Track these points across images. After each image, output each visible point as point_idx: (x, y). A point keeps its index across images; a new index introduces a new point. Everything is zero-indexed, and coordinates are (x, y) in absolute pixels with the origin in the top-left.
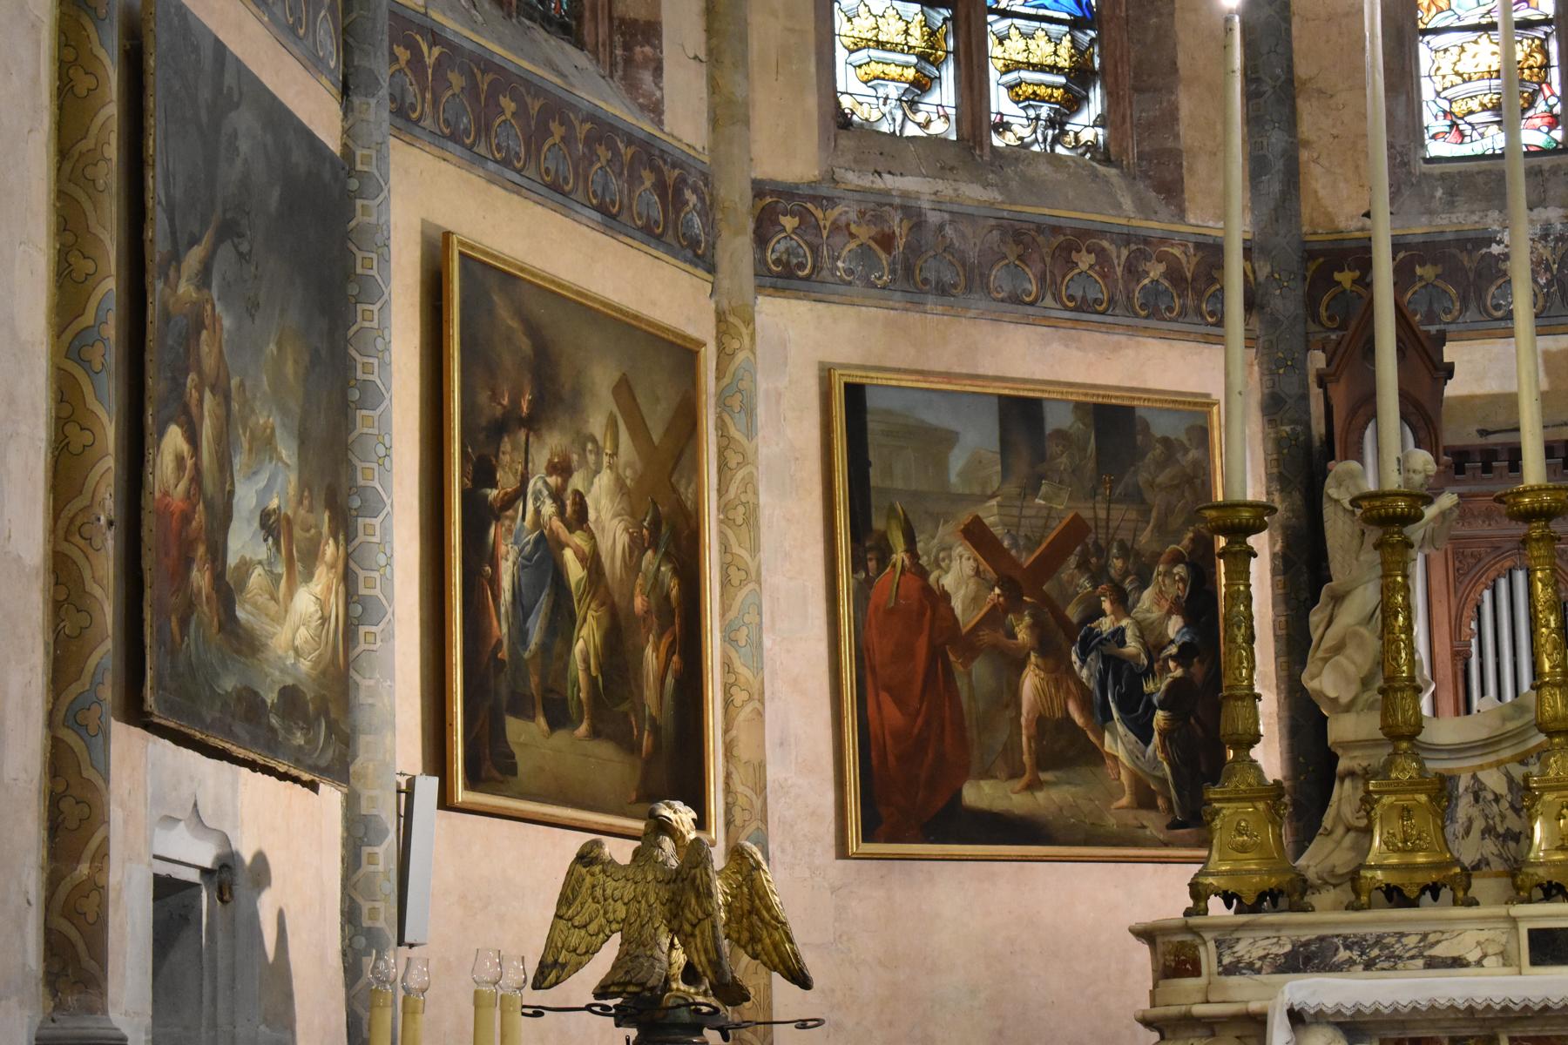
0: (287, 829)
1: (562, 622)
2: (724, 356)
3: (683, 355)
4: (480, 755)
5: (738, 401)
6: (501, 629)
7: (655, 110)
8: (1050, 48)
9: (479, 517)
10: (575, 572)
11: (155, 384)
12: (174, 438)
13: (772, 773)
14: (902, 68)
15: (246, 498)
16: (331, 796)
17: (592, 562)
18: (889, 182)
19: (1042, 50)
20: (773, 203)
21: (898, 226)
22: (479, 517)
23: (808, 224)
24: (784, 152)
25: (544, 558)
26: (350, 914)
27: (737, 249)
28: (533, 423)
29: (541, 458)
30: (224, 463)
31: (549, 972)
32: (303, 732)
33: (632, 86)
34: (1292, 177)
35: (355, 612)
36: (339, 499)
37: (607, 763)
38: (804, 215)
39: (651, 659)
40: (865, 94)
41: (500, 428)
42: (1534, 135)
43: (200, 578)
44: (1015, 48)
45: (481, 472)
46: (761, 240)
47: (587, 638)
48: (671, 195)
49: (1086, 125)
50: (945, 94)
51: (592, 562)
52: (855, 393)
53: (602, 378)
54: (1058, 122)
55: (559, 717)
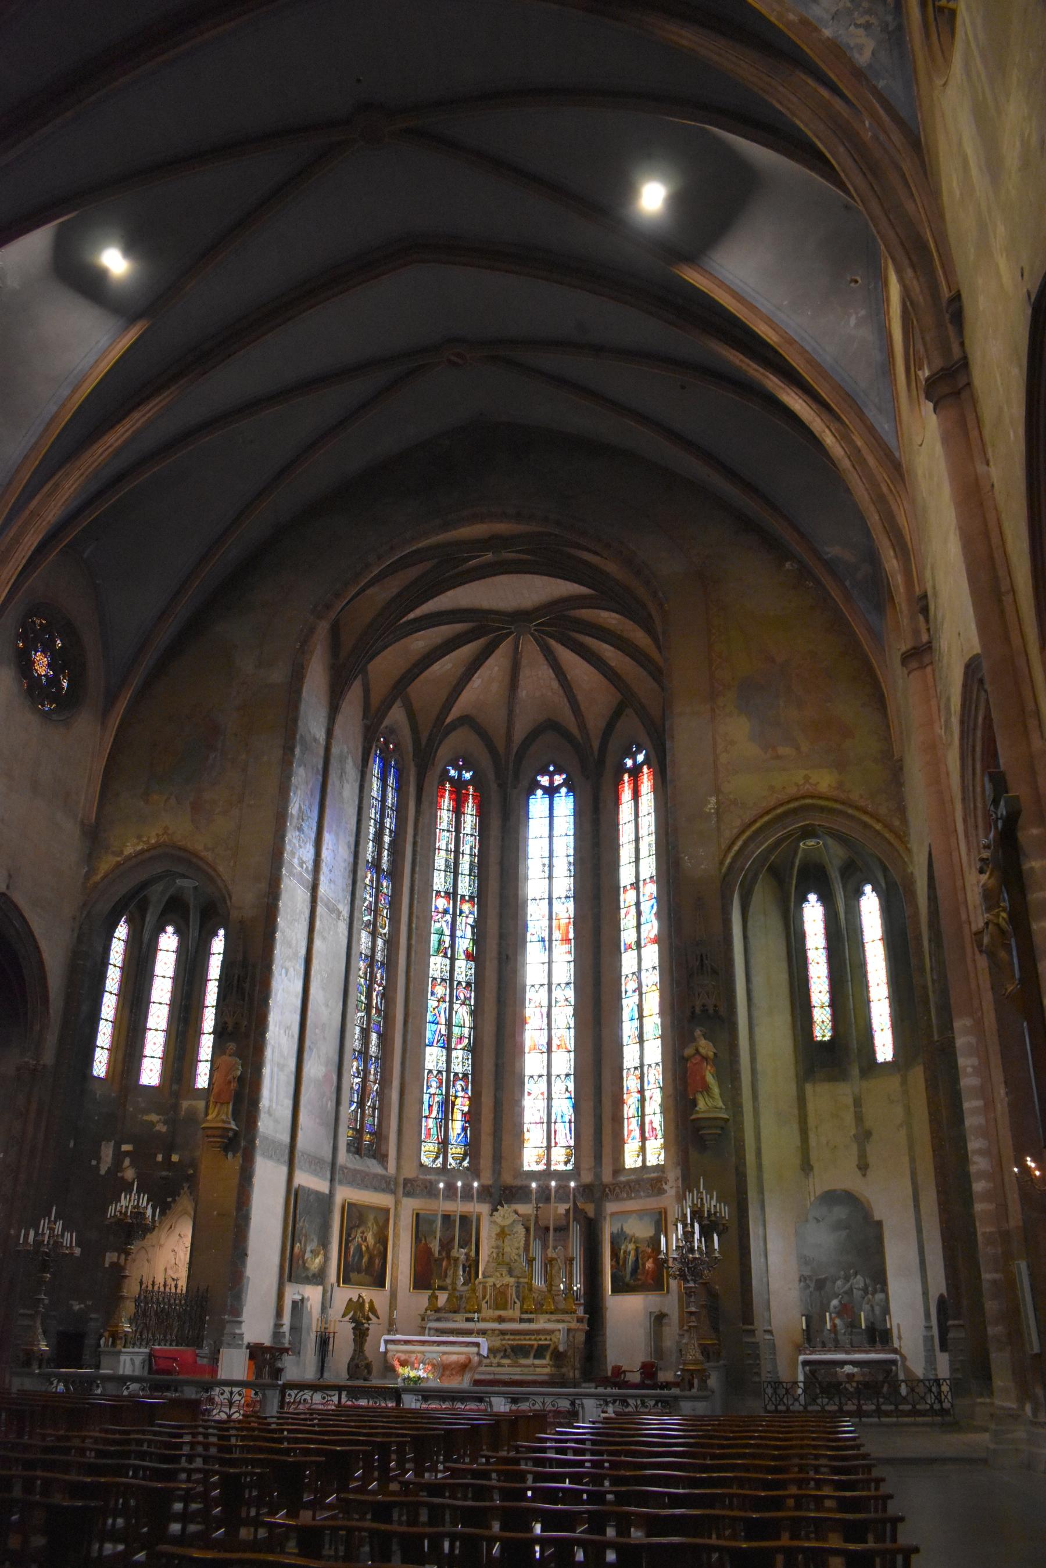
0: (313, 1294)
1: (361, 1256)
2: (396, 1209)
3: (388, 1211)
4: (345, 1279)
5: (397, 1216)
6: (350, 1259)
7: (386, 1169)
8: (460, 1150)
9: (348, 1242)
10: (364, 1248)
11: (296, 1239)
12: (298, 1244)
13: (399, 1277)
14: (433, 1155)
15: (308, 1249)
16: (320, 1288)
17: (367, 1247)
18: (428, 1177)
19: (458, 1150)
20: (406, 1181)
21: (428, 1185)
22: (348, 1242)
23: (412, 1185)
24: (409, 1172)
25: (359, 1246)
26: (323, 1304)
27: (401, 1190)
28: (358, 1226)
29: (360, 1231)
30: (305, 1246)
31: (343, 1316)
32: (318, 1278)
33: (383, 1166)
34: (499, 1174)
35: (327, 1259)
36: (324, 1243)
37: (368, 1279)
38: (412, 1185)
39: (377, 1261)
40: (426, 1160)
41: (352, 1228)
42: (542, 1167)
43: (301, 1262)
44: (454, 1151)
45: (349, 1235)
46: (404, 1188)
47: (365, 1260)
48: (388, 1183)
49: (466, 1164)
50: (441, 1159)
51: (367, 1247)
52: (418, 1215)
53: (371, 1217)
54: (460, 1163)
55: (359, 1272)
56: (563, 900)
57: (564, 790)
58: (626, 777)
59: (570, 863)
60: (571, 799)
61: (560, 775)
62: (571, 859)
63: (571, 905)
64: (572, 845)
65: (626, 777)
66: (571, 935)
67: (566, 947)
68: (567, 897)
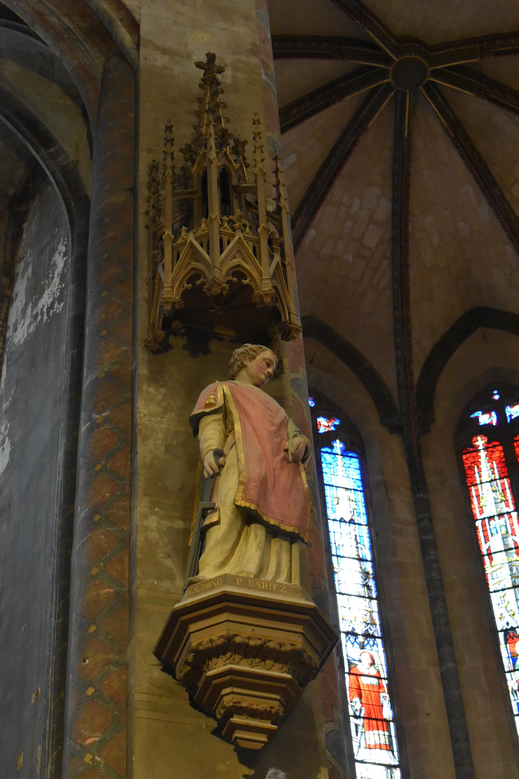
56: (361, 639)
57: (338, 445)
58: (480, 442)
59: (366, 574)
60: (355, 463)
61: (329, 418)
62: (368, 567)
63: (378, 651)
64: (366, 541)
65: (480, 442)
66: (387, 713)
67: (377, 736)
68: (367, 635)
